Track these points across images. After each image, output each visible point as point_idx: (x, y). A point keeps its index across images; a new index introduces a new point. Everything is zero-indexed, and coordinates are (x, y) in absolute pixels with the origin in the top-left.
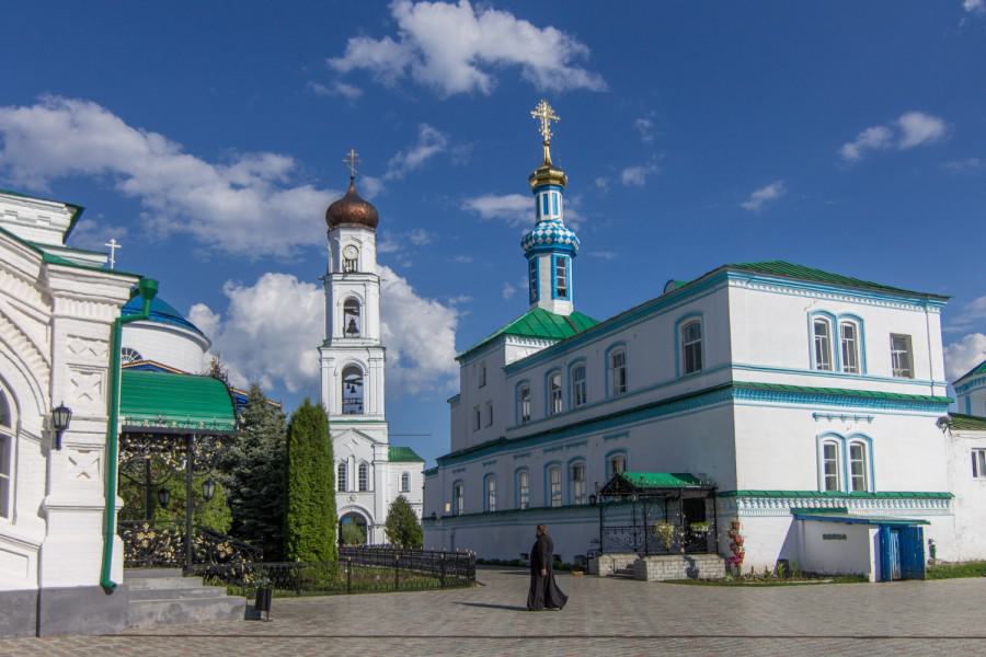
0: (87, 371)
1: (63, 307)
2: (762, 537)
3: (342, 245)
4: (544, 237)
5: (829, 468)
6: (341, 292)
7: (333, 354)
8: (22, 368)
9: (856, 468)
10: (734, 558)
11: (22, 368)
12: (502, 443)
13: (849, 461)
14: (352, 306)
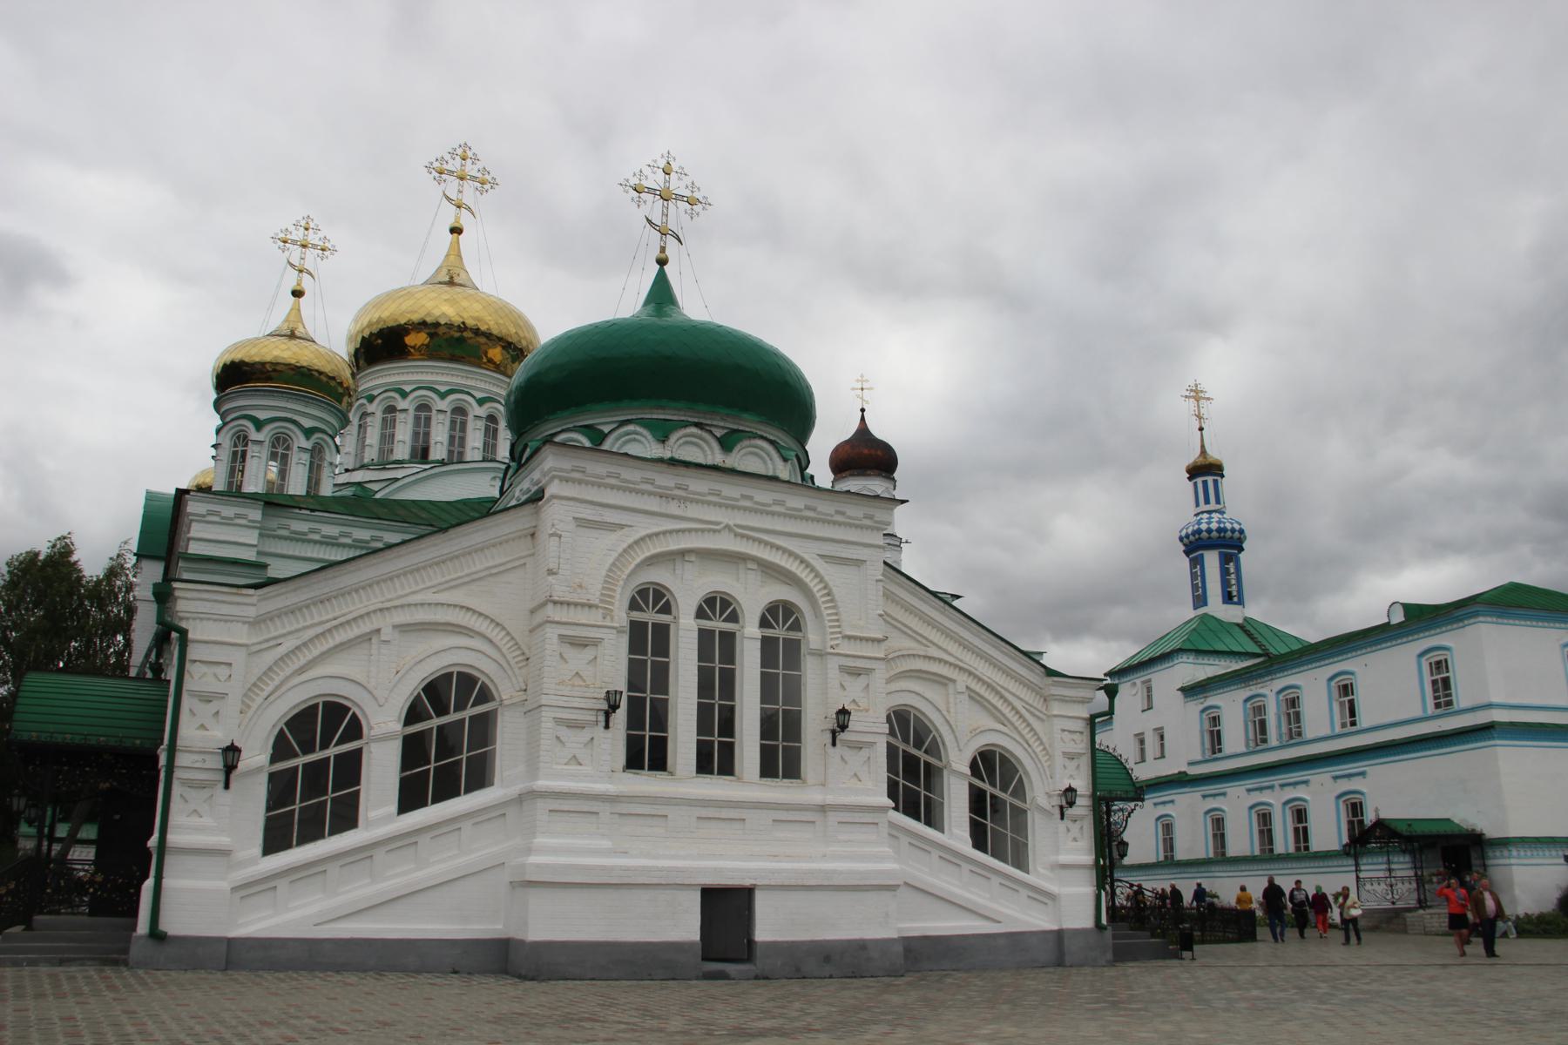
4: (1209, 531)
11: (1034, 757)
12: (1180, 781)
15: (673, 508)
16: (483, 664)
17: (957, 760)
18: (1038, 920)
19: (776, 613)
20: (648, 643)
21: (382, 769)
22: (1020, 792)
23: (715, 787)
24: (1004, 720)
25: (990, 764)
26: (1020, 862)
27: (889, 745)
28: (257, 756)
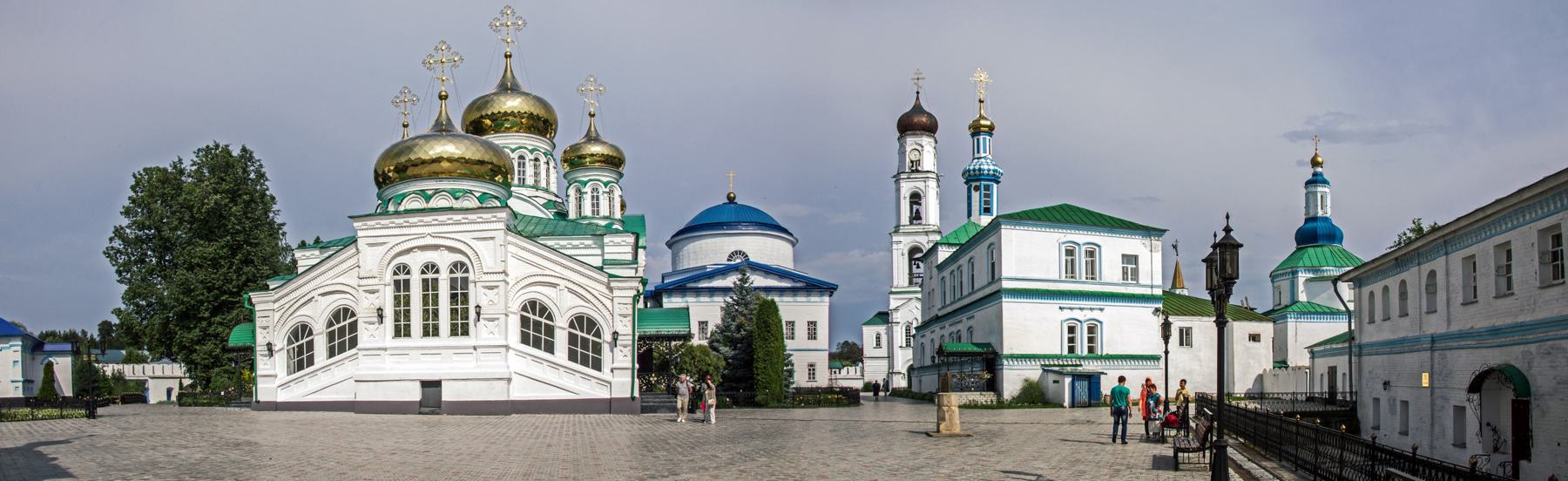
0: (625, 316)
1: (616, 293)
2: (1013, 380)
3: (908, 149)
5: (1071, 340)
6: (907, 188)
7: (901, 238)
8: (604, 317)
9: (1091, 340)
10: (999, 393)
11: (604, 317)
13: (1086, 335)
14: (916, 198)
15: (405, 231)
16: (351, 304)
17: (561, 323)
18: (603, 394)
19: (457, 266)
20: (402, 286)
21: (321, 345)
22: (598, 334)
23: (431, 341)
24: (588, 301)
25: (580, 321)
26: (597, 366)
27: (523, 317)
28: (280, 343)
